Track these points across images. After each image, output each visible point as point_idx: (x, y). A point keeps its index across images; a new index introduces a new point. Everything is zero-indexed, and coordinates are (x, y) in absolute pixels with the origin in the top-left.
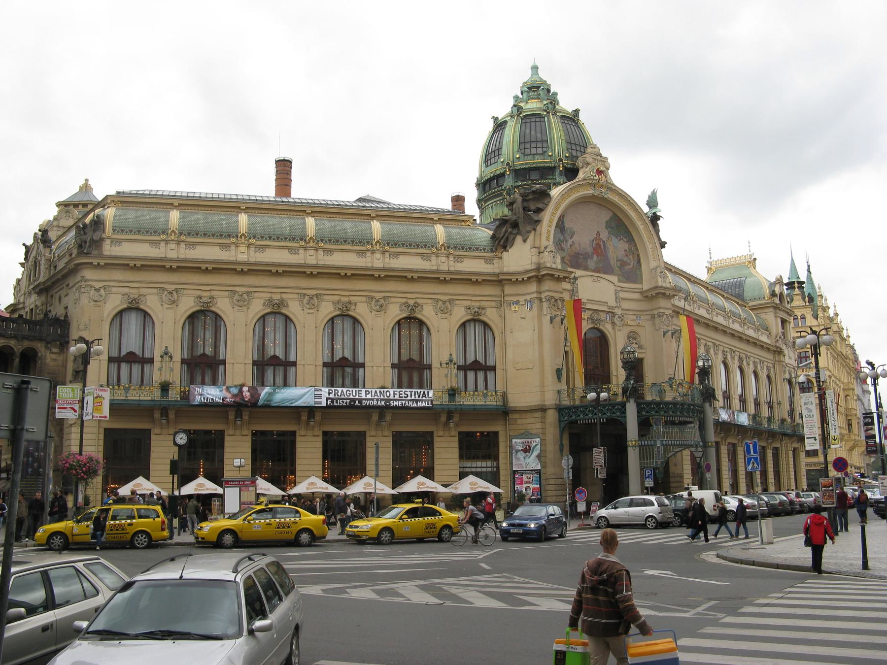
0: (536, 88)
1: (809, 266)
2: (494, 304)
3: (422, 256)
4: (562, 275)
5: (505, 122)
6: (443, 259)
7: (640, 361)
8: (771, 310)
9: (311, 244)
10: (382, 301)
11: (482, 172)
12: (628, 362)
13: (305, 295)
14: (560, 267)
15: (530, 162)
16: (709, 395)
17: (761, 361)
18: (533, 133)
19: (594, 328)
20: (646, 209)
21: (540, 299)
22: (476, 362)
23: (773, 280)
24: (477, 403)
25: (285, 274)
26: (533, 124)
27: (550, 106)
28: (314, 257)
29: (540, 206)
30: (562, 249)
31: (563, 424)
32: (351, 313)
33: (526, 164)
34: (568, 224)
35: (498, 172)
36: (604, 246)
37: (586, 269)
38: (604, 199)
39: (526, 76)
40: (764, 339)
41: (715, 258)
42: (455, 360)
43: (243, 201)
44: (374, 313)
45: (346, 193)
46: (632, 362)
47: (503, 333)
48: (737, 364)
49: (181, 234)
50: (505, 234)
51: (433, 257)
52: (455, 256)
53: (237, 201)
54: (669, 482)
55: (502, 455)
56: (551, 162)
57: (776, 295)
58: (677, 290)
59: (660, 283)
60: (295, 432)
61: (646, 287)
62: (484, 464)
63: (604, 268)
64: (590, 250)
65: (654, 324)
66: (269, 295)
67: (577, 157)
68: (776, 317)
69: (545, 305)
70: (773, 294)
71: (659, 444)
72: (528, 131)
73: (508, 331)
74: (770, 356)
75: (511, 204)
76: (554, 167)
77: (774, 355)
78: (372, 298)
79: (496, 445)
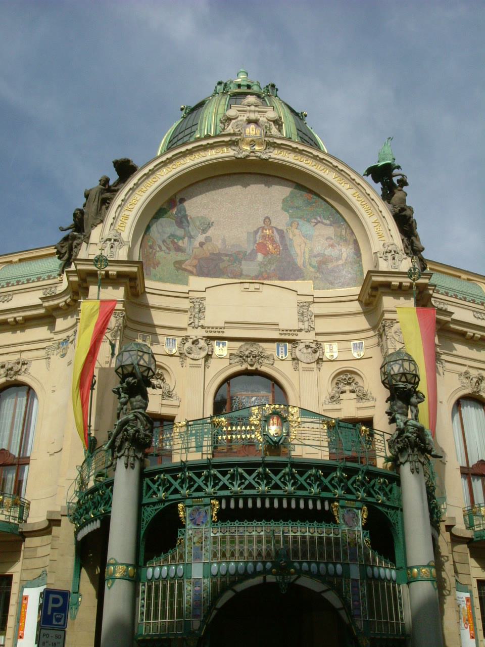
2: (42, 353)
19: (246, 373)
30: (179, 249)
38: (265, 162)
46: (132, 374)
59: (384, 266)
71: (197, 571)
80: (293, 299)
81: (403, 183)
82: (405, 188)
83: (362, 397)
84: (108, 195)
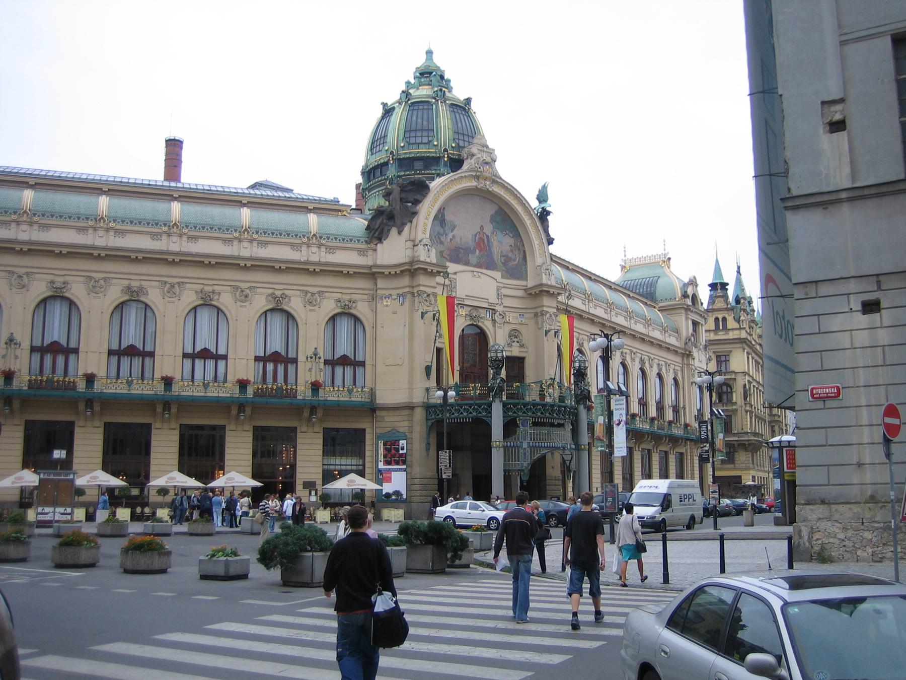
0: (428, 74)
1: (739, 268)
2: (365, 297)
3: (292, 245)
4: (435, 270)
5: (393, 108)
6: (314, 249)
7: (521, 360)
8: (683, 311)
9: (175, 229)
10: (248, 291)
11: (367, 160)
12: (495, 361)
13: (166, 283)
14: (434, 261)
15: (414, 151)
16: (583, 397)
17: (666, 363)
18: (419, 120)
19: (472, 325)
20: (534, 204)
21: (413, 294)
22: (345, 357)
23: (686, 280)
24: (341, 399)
25: (145, 260)
26: (425, 112)
27: (439, 93)
28: (177, 244)
29: (418, 197)
30: (442, 243)
31: (430, 423)
32: (213, 303)
33: (410, 153)
34: (448, 217)
35: (382, 161)
36: (488, 240)
37: (467, 263)
39: (420, 61)
40: (672, 340)
41: (629, 256)
42: (321, 354)
43: (107, 182)
44: (239, 303)
45: (238, 181)
46: (499, 360)
47: (375, 327)
48: (637, 366)
49: (35, 215)
50: (380, 226)
51: (304, 248)
52: (327, 247)
53: (100, 182)
54: (545, 485)
55: (368, 453)
56: (436, 152)
57: (688, 297)
58: (563, 288)
60: (151, 424)
61: (530, 283)
62: (349, 462)
63: (488, 264)
64: (472, 244)
65: (537, 322)
66: (126, 282)
67: (464, 147)
68: (687, 318)
69: (416, 299)
70: (685, 295)
71: (525, 445)
72: (414, 118)
73: (379, 327)
74: (679, 359)
75: (387, 195)
76: (439, 157)
77: (683, 358)
78: (237, 288)
79: (363, 442)
80: (495, 284)
81: (548, 213)
82: (548, 217)
83: (522, 346)
84: (403, 195)
